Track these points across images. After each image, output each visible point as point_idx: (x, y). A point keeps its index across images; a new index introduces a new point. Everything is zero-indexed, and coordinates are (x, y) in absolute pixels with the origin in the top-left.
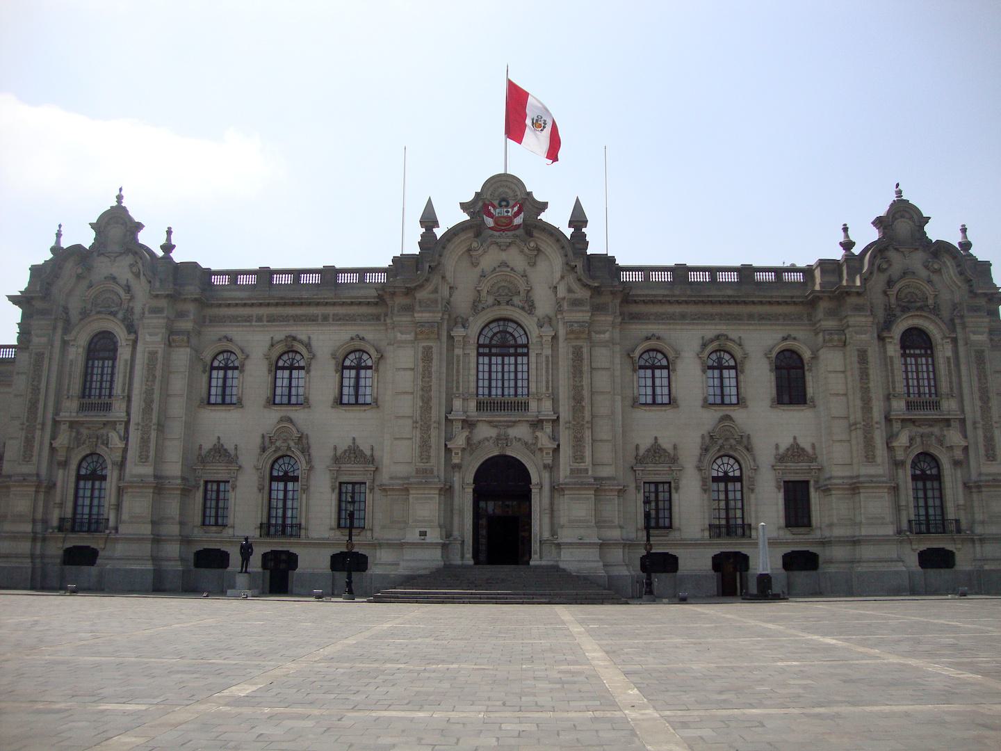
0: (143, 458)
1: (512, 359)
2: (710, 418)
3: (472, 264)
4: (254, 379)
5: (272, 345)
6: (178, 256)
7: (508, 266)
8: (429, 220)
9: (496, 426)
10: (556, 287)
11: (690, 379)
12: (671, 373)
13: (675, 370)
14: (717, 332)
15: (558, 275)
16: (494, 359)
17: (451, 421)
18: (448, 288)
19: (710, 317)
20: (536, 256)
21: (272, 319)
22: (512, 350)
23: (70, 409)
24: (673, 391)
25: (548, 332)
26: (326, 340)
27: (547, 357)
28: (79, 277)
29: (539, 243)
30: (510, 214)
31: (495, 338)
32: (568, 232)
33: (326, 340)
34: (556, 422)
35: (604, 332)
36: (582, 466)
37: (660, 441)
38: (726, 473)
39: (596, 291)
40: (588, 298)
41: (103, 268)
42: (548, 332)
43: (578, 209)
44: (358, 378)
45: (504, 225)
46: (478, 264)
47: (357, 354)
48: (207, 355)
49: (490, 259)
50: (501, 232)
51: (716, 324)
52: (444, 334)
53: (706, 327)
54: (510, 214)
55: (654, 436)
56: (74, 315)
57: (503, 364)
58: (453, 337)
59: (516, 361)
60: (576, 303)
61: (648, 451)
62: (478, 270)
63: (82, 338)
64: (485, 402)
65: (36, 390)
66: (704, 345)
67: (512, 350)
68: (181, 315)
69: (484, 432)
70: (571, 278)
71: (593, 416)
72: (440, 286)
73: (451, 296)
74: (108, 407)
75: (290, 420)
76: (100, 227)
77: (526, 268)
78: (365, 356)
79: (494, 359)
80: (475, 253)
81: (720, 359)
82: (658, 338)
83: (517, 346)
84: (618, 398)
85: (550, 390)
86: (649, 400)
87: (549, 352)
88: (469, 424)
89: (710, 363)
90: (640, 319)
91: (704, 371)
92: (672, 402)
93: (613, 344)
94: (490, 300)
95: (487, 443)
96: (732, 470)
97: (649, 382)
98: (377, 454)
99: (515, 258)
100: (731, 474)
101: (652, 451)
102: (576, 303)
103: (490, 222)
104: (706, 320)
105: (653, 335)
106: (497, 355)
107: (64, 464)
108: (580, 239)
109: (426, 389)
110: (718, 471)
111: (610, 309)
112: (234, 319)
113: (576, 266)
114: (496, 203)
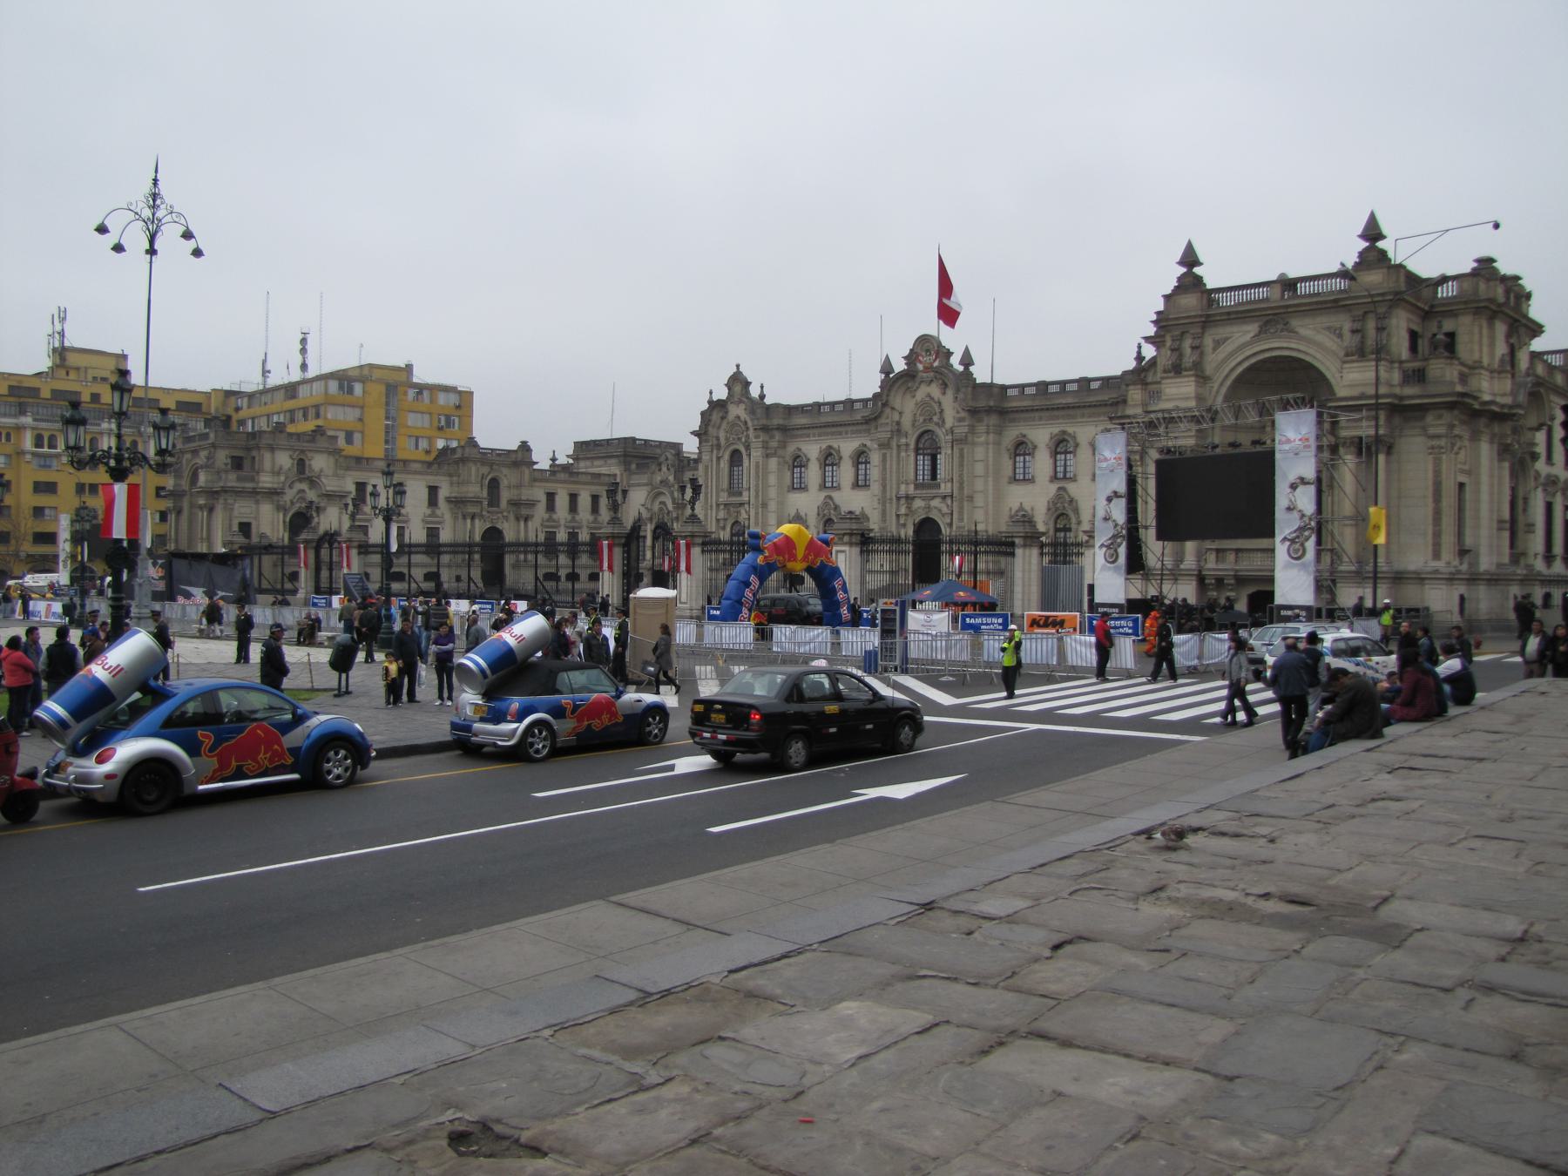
0: (757, 524)
2: (1053, 489)
4: (813, 473)
6: (768, 401)
8: (887, 368)
11: (1042, 464)
19: (1057, 418)
23: (724, 497)
25: (949, 437)
28: (723, 418)
33: (848, 446)
39: (973, 412)
42: (949, 437)
48: (789, 459)
49: (921, 393)
56: (723, 441)
60: (961, 420)
68: (772, 437)
69: (918, 503)
74: (740, 494)
75: (830, 498)
76: (729, 385)
88: (909, 499)
92: (1032, 481)
99: (935, 390)
102: (961, 420)
103: (920, 367)
107: (724, 528)
108: (967, 375)
109: (884, 479)
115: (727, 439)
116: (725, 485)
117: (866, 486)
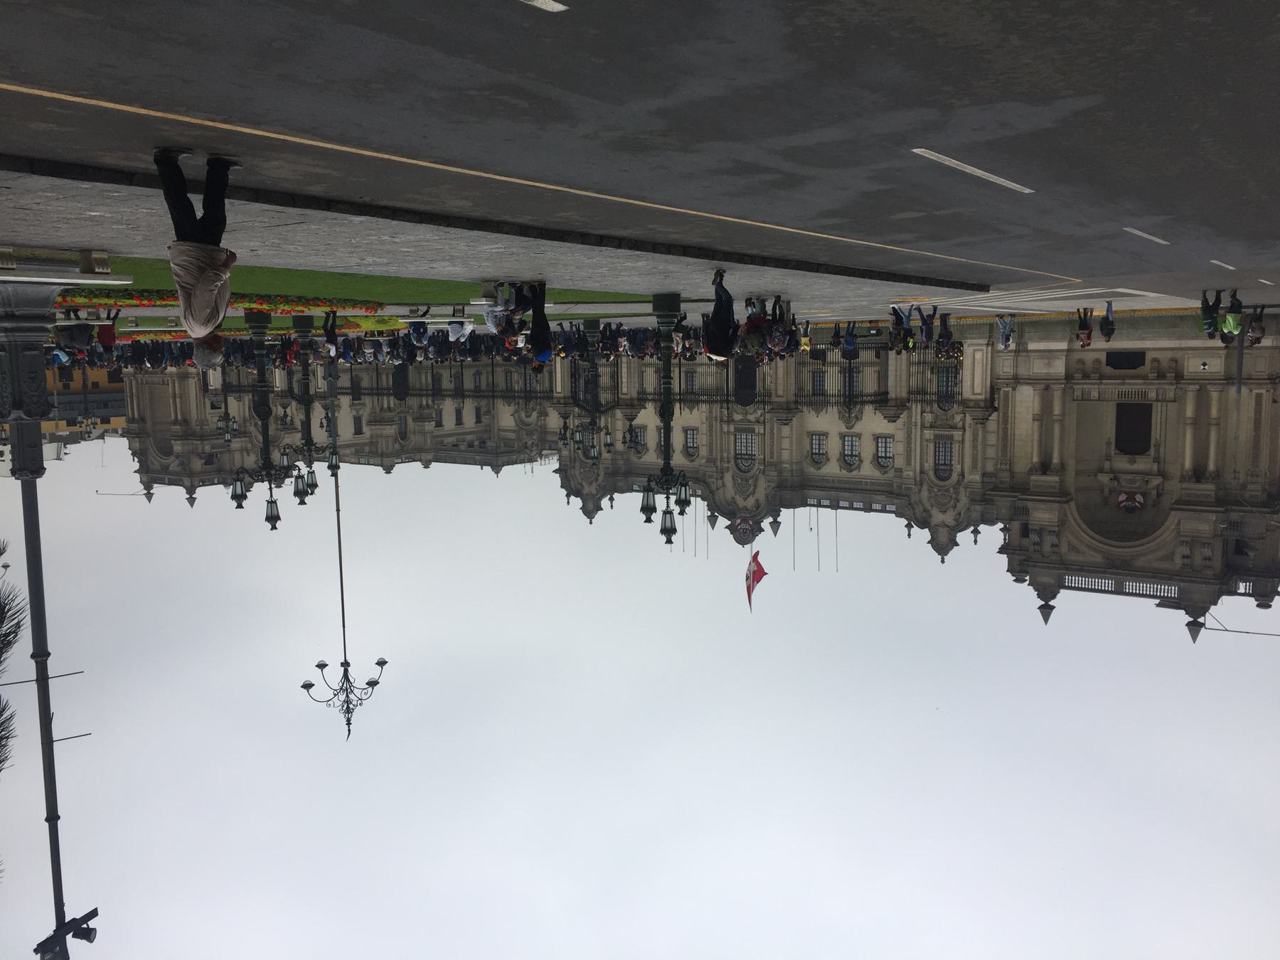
5: (859, 468)
15: (721, 491)
21: (860, 483)
23: (957, 435)
26: (832, 469)
39: (704, 482)
41: (949, 518)
45: (744, 520)
49: (750, 502)
63: (955, 477)
65: (975, 447)
68: (900, 487)
70: (714, 487)
74: (936, 436)
88: (758, 421)
99: (740, 501)
102: (711, 477)
112: (880, 485)
115: (957, 493)
116: (956, 447)
117: (811, 435)
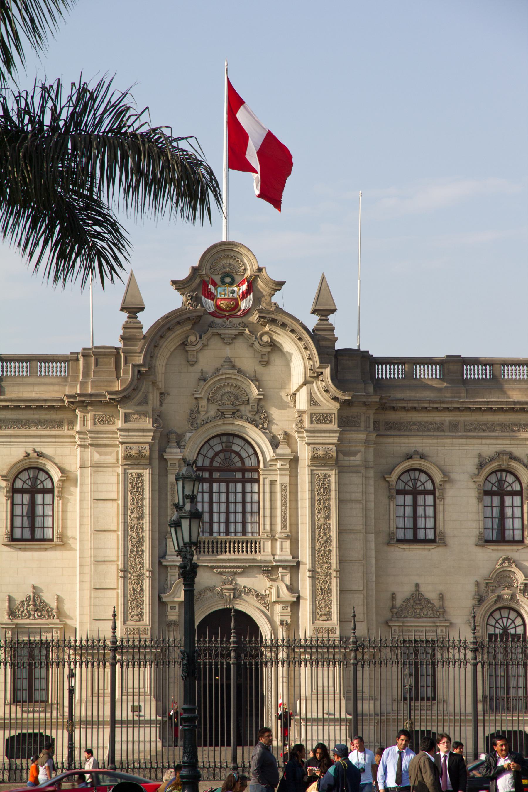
1: (239, 486)
3: (188, 362)
7: (234, 367)
9: (221, 573)
10: (295, 394)
12: (437, 501)
13: (442, 498)
14: (499, 448)
16: (215, 486)
17: (166, 567)
18: (158, 395)
19: (490, 427)
20: (269, 352)
22: (239, 475)
24: (440, 524)
27: (283, 485)
29: (274, 337)
30: (235, 295)
31: (218, 459)
32: (312, 322)
34: (294, 568)
35: (354, 454)
36: (328, 624)
37: (422, 589)
38: (505, 630)
40: (336, 412)
43: (323, 289)
44: (33, 504)
46: (196, 362)
47: (32, 473)
49: (211, 356)
50: (225, 319)
51: (497, 438)
52: (156, 455)
53: (484, 441)
54: (235, 295)
55: (415, 582)
57: (227, 493)
58: (165, 460)
59: (244, 488)
61: (407, 600)
62: (194, 372)
64: (206, 541)
66: (481, 465)
67: (239, 475)
71: (341, 561)
72: (150, 397)
73: (161, 405)
77: (256, 368)
78: (42, 476)
79: (215, 486)
80: (192, 349)
81: (501, 482)
82: (423, 457)
83: (243, 471)
84: (372, 537)
85: (288, 530)
86: (410, 535)
87: (286, 479)
89: (488, 487)
90: (399, 430)
91: (480, 499)
92: (437, 540)
93: (366, 468)
94: (212, 411)
95: (209, 594)
96: (513, 626)
97: (409, 511)
98: (67, 607)
100: (512, 631)
101: (412, 601)
103: (210, 304)
104: (484, 431)
105: (416, 452)
106: (219, 481)
110: (495, 627)
111: (363, 424)
113: (322, 373)
114: (217, 279)
